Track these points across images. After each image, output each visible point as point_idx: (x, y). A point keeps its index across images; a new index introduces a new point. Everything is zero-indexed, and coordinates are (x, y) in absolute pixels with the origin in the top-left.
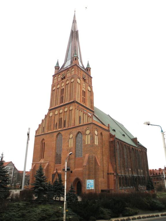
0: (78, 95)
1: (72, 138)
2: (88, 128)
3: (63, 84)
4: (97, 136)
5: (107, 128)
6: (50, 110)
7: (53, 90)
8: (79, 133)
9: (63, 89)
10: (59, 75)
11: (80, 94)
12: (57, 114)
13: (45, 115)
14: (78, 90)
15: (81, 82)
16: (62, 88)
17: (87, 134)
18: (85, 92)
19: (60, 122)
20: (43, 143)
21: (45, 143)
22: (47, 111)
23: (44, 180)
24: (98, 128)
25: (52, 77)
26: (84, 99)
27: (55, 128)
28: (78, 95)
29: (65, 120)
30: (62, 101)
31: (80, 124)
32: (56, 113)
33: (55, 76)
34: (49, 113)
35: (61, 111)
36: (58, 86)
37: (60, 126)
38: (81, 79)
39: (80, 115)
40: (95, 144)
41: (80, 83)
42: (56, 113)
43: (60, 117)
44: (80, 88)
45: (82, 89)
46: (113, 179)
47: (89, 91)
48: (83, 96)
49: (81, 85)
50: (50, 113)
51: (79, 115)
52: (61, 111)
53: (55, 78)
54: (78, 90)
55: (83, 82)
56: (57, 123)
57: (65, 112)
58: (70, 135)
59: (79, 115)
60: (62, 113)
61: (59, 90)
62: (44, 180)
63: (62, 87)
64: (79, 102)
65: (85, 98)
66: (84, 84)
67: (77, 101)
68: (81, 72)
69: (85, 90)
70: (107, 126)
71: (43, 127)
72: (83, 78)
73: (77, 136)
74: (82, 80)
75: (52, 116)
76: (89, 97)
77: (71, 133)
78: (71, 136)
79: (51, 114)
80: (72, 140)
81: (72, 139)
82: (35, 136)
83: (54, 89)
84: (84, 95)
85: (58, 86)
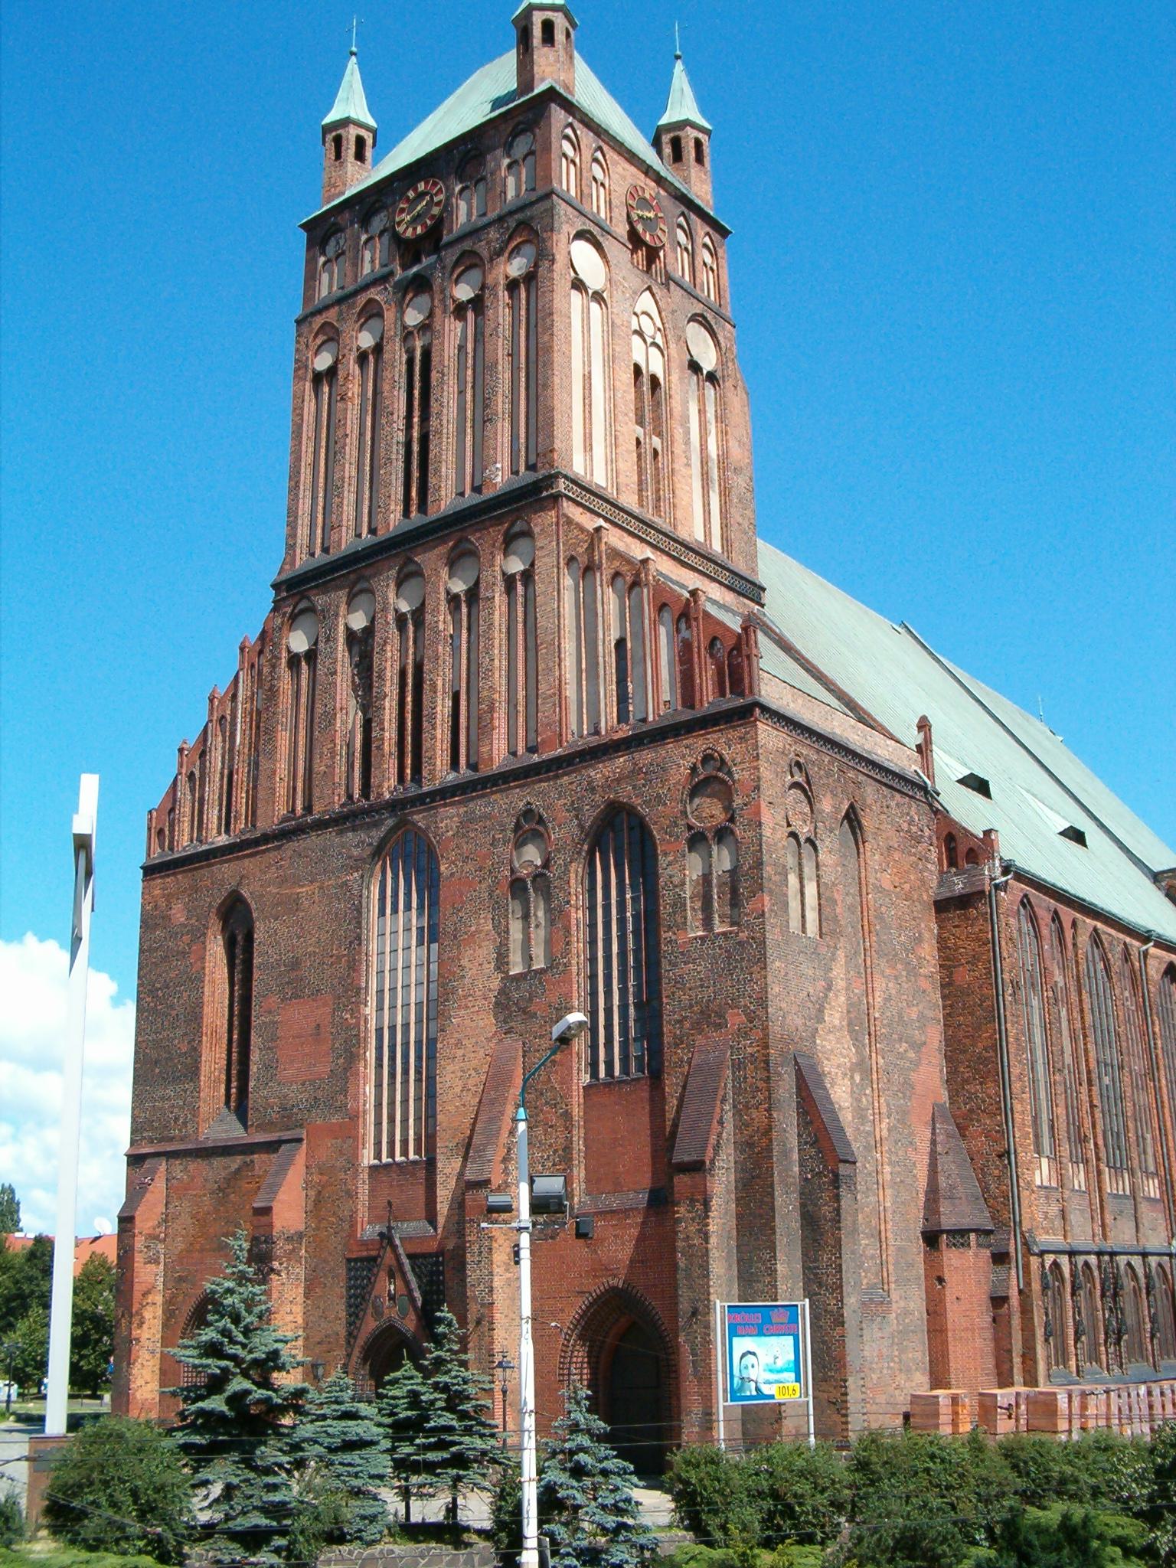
5: (907, 763)
26: (649, 458)
38: (607, 243)
44: (607, 345)
48: (640, 422)
65: (656, 442)
66: (646, 302)
67: (578, 467)
69: (656, 365)
70: (914, 738)
74: (619, 253)
82: (150, 871)
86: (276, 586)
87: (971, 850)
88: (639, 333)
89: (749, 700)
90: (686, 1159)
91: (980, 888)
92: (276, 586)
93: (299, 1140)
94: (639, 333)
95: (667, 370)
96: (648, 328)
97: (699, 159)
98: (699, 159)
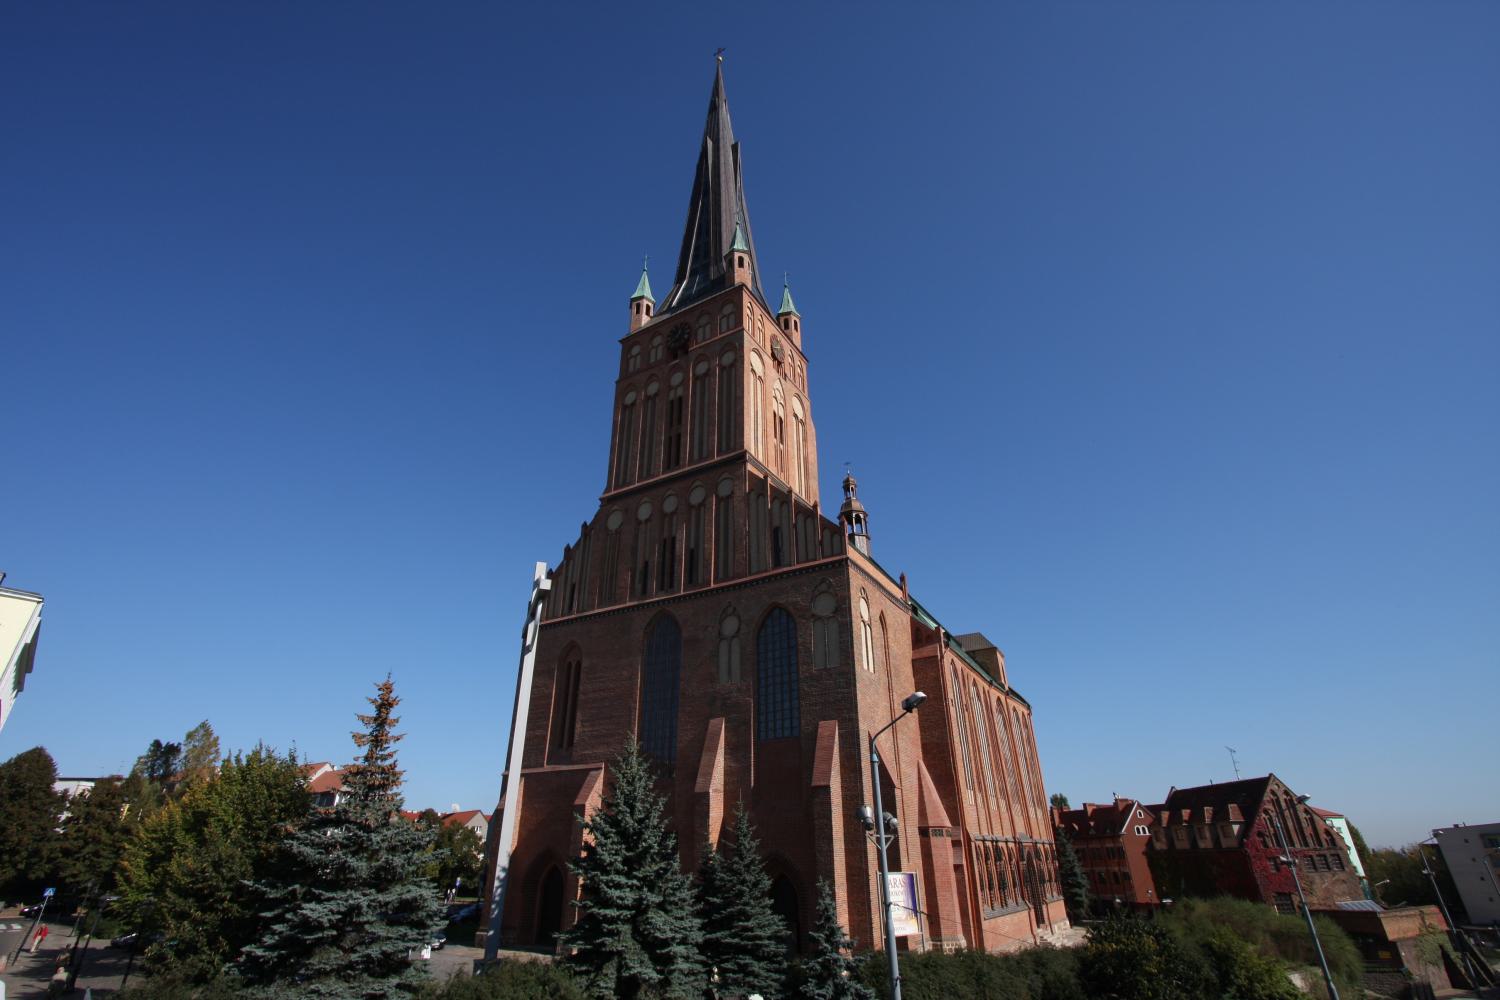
0: (756, 430)
1: (733, 637)
2: (824, 587)
3: (677, 378)
4: (868, 628)
6: (607, 502)
7: (625, 407)
8: (777, 612)
9: (680, 399)
10: (652, 339)
11: (765, 431)
12: (647, 521)
13: (585, 525)
14: (756, 405)
15: (767, 372)
16: (672, 395)
17: (820, 618)
18: (781, 419)
21: (579, 665)
22: (596, 507)
23: (640, 888)
24: (870, 587)
27: (638, 586)
28: (756, 430)
29: (692, 546)
30: (673, 460)
31: (777, 563)
32: (644, 512)
33: (636, 343)
35: (670, 505)
36: (653, 388)
37: (667, 580)
38: (765, 357)
39: (776, 523)
40: (865, 667)
41: (761, 374)
42: (644, 512)
43: (666, 535)
45: (771, 405)
46: (951, 862)
47: (796, 416)
48: (776, 437)
49: (767, 384)
50: (608, 516)
52: (670, 505)
53: (636, 350)
54: (756, 405)
55: (772, 372)
56: (646, 563)
57: (692, 507)
59: (771, 523)
60: (673, 513)
61: (654, 403)
62: (640, 888)
63: (670, 388)
64: (760, 459)
65: (781, 446)
66: (777, 385)
68: (763, 325)
72: (773, 355)
74: (769, 361)
76: (799, 449)
77: (730, 610)
78: (730, 625)
79: (614, 521)
80: (736, 648)
81: (735, 641)
83: (630, 398)
84: (778, 436)
85: (653, 388)
86: (601, 499)
89: (844, 557)
90: (818, 784)
91: (932, 654)
92: (601, 499)
93: (601, 768)
95: (786, 415)
96: (779, 397)
97: (796, 328)
98: (796, 328)
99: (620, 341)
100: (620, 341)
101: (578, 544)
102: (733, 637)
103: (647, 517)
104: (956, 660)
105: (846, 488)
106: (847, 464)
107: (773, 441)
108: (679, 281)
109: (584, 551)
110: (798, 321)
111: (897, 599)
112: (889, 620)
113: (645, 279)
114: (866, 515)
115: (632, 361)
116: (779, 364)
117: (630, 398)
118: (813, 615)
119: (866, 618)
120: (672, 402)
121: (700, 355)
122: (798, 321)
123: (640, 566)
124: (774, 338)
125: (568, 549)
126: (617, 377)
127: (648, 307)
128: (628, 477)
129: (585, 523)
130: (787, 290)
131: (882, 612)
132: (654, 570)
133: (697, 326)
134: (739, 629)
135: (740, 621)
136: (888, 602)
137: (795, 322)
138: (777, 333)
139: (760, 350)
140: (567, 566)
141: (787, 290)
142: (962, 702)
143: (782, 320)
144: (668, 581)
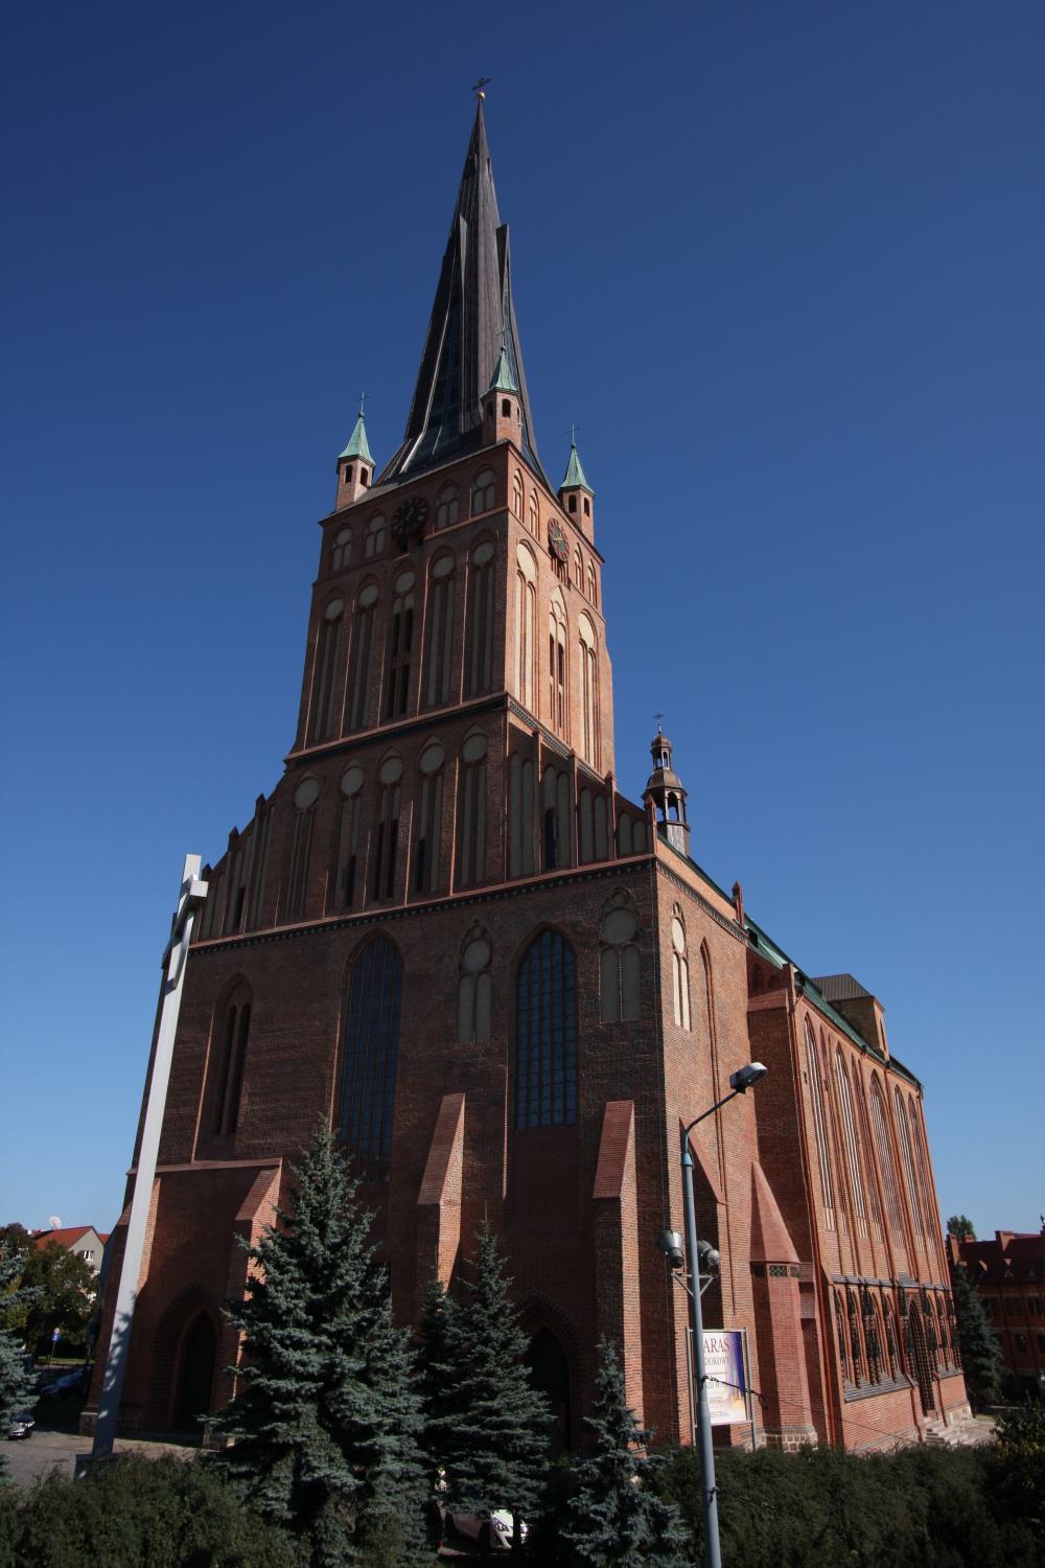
1: (481, 973)
2: (619, 900)
3: (405, 581)
4: (683, 963)
6: (295, 765)
7: (326, 623)
8: (548, 935)
9: (410, 613)
10: (370, 520)
11: (536, 664)
12: (356, 795)
15: (542, 576)
16: (397, 608)
17: (611, 947)
18: (560, 646)
19: (386, 849)
20: (234, 1010)
21: (247, 1009)
22: (278, 772)
23: (331, 1349)
24: (688, 904)
25: (321, 529)
27: (340, 894)
29: (423, 834)
30: (397, 703)
31: (550, 863)
32: (352, 782)
34: (285, 789)
36: (369, 595)
37: (383, 884)
39: (549, 803)
42: (352, 782)
43: (383, 817)
45: (547, 626)
46: (798, 1315)
47: (583, 643)
48: (552, 674)
49: (542, 593)
50: (296, 788)
51: (542, 801)
52: (390, 773)
53: (344, 537)
55: (549, 577)
56: (353, 860)
57: (425, 775)
58: (463, 952)
59: (542, 801)
60: (396, 785)
62: (331, 1349)
63: (395, 596)
64: (528, 706)
65: (560, 688)
66: (556, 596)
68: (537, 505)
69: (561, 639)
71: (242, 891)
73: (525, 956)
74: (545, 560)
75: (311, 811)
76: (586, 694)
77: (478, 932)
78: (477, 956)
79: (306, 795)
80: (485, 991)
81: (485, 982)
83: (333, 610)
85: (369, 595)
86: (287, 762)
87: (773, 977)
88: (553, 615)
89: (650, 856)
90: (603, 1195)
91: (778, 1005)
92: (287, 762)
93: (278, 1166)
94: (553, 615)
95: (568, 641)
96: (558, 615)
97: (587, 511)
98: (587, 511)
99: (320, 523)
100: (320, 523)
101: (250, 828)
102: (481, 973)
103: (355, 789)
104: (813, 1014)
105: (657, 753)
106: (658, 716)
107: (547, 680)
108: (412, 434)
109: (259, 837)
110: (590, 499)
111: (727, 922)
112: (715, 952)
113: (361, 429)
114: (684, 794)
115: (338, 553)
116: (561, 563)
117: (333, 610)
118: (602, 943)
119: (680, 949)
120: (398, 616)
121: (443, 546)
122: (590, 499)
123: (343, 863)
124: (552, 524)
125: (234, 835)
126: (315, 577)
127: (364, 472)
128: (328, 729)
129: (262, 796)
130: (574, 453)
131: (704, 940)
132: (365, 870)
133: (438, 503)
134: (490, 961)
135: (491, 945)
136: (714, 924)
137: (586, 501)
138: (558, 517)
139: (533, 543)
140: (234, 860)
141: (574, 453)
142: (819, 1075)
143: (566, 497)
144: (384, 889)
